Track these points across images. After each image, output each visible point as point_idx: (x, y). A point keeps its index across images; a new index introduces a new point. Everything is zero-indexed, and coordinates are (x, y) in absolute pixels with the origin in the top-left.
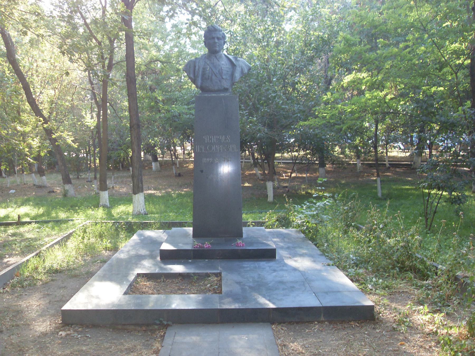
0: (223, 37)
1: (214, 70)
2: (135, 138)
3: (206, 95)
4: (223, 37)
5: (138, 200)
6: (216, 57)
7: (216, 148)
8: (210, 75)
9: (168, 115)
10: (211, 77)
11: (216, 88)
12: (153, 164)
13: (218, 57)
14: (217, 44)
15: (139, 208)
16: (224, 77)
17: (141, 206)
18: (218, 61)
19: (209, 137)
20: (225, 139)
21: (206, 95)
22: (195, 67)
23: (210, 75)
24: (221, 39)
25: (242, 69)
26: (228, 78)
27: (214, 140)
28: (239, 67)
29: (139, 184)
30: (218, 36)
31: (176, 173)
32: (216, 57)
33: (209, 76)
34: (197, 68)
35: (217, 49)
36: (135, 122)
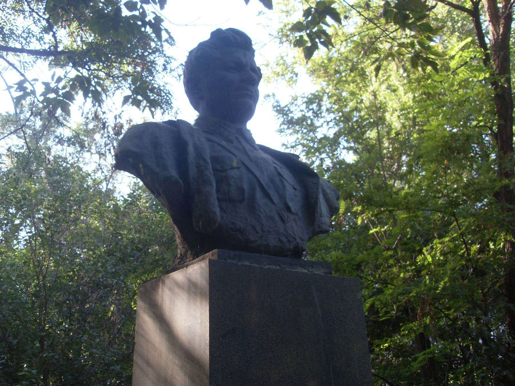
10: (252, 198)
11: (272, 241)
33: (241, 190)
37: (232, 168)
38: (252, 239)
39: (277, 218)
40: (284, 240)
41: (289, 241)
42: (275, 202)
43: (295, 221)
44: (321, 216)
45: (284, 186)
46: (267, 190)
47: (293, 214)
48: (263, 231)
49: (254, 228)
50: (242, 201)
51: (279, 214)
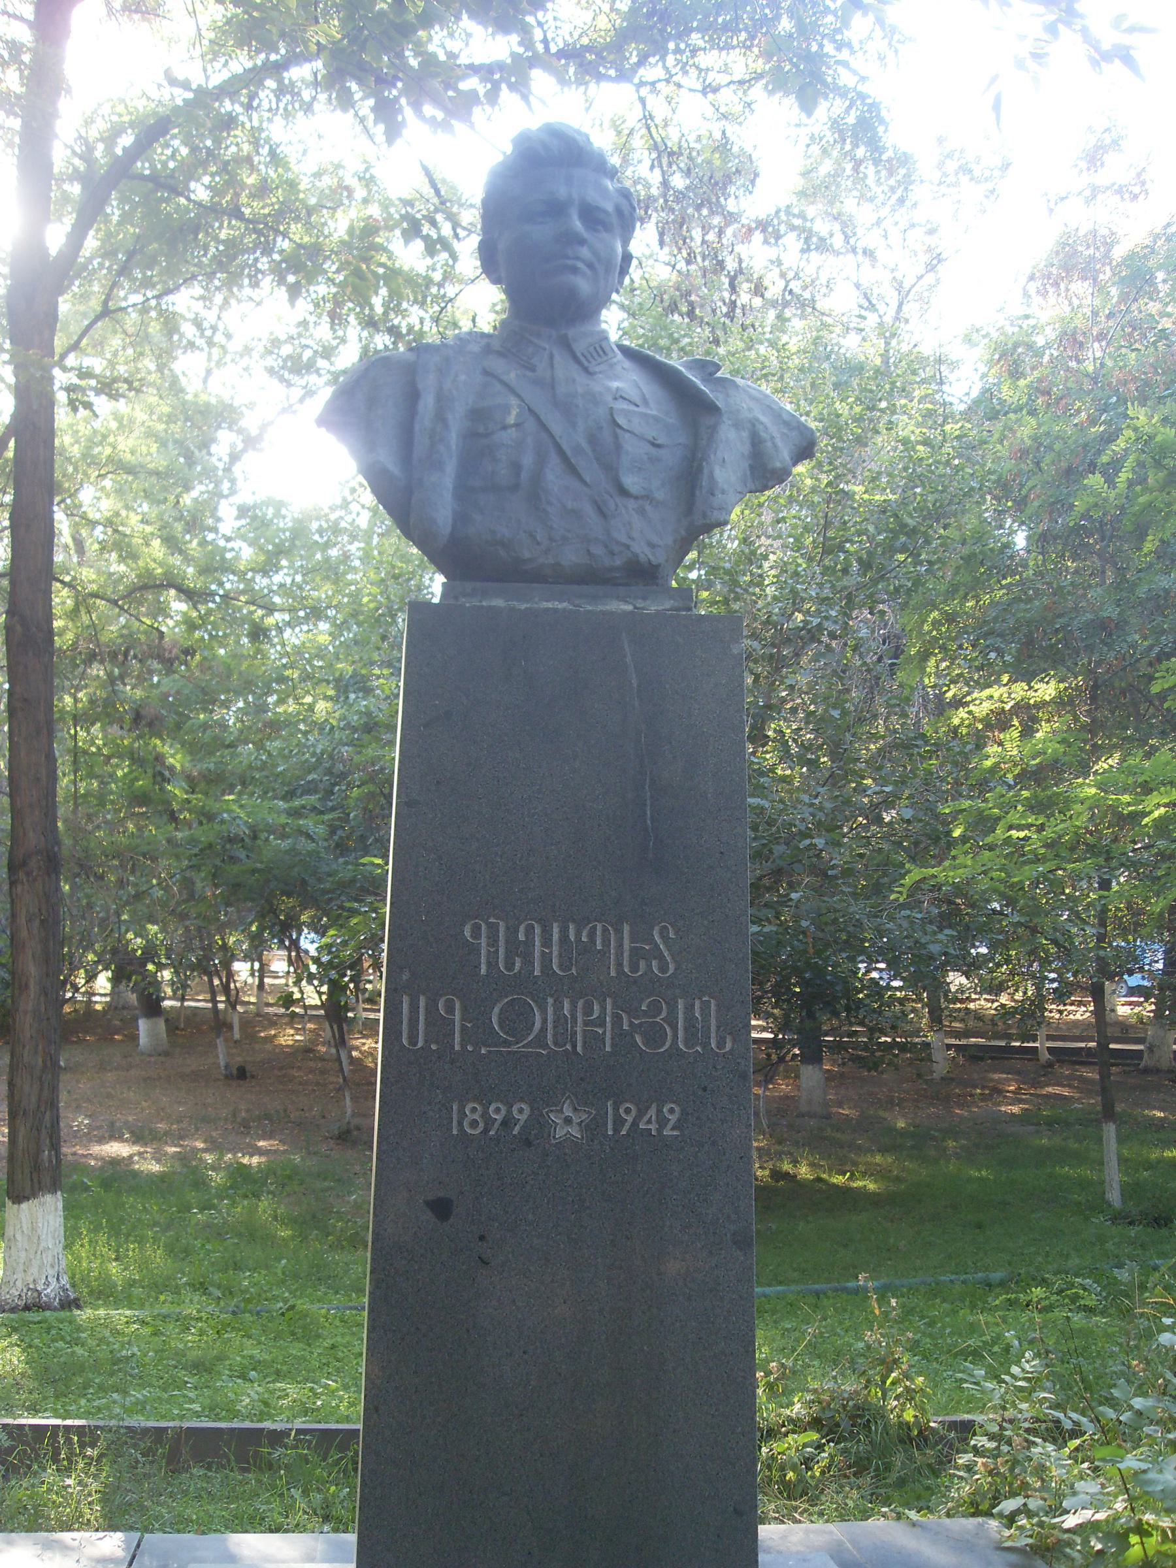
0: (619, 212)
1: (557, 427)
2: (29, 920)
3: (499, 603)
4: (619, 212)
5: (33, 1229)
6: (566, 345)
7: (559, 1020)
8: (528, 460)
9: (205, 834)
10: (537, 478)
11: (571, 557)
12: (143, 1025)
13: (579, 347)
14: (585, 252)
15: (34, 1270)
16: (631, 481)
17: (48, 1258)
18: (586, 370)
19: (512, 931)
21: (499, 603)
22: (413, 396)
23: (528, 460)
24: (608, 228)
25: (756, 441)
26: (660, 495)
27: (546, 959)
28: (737, 425)
29: (39, 1151)
30: (593, 197)
31: (226, 1067)
32: (566, 345)
33: (516, 467)
34: (427, 403)
35: (583, 285)
36: (33, 839)
37: (505, 428)
38: (527, 555)
39: (589, 510)
40: (598, 550)
41: (612, 553)
42: (588, 479)
43: (642, 512)
44: (713, 494)
45: (618, 447)
46: (573, 461)
47: (636, 498)
48: (551, 539)
49: (531, 536)
50: (515, 488)
51: (595, 502)
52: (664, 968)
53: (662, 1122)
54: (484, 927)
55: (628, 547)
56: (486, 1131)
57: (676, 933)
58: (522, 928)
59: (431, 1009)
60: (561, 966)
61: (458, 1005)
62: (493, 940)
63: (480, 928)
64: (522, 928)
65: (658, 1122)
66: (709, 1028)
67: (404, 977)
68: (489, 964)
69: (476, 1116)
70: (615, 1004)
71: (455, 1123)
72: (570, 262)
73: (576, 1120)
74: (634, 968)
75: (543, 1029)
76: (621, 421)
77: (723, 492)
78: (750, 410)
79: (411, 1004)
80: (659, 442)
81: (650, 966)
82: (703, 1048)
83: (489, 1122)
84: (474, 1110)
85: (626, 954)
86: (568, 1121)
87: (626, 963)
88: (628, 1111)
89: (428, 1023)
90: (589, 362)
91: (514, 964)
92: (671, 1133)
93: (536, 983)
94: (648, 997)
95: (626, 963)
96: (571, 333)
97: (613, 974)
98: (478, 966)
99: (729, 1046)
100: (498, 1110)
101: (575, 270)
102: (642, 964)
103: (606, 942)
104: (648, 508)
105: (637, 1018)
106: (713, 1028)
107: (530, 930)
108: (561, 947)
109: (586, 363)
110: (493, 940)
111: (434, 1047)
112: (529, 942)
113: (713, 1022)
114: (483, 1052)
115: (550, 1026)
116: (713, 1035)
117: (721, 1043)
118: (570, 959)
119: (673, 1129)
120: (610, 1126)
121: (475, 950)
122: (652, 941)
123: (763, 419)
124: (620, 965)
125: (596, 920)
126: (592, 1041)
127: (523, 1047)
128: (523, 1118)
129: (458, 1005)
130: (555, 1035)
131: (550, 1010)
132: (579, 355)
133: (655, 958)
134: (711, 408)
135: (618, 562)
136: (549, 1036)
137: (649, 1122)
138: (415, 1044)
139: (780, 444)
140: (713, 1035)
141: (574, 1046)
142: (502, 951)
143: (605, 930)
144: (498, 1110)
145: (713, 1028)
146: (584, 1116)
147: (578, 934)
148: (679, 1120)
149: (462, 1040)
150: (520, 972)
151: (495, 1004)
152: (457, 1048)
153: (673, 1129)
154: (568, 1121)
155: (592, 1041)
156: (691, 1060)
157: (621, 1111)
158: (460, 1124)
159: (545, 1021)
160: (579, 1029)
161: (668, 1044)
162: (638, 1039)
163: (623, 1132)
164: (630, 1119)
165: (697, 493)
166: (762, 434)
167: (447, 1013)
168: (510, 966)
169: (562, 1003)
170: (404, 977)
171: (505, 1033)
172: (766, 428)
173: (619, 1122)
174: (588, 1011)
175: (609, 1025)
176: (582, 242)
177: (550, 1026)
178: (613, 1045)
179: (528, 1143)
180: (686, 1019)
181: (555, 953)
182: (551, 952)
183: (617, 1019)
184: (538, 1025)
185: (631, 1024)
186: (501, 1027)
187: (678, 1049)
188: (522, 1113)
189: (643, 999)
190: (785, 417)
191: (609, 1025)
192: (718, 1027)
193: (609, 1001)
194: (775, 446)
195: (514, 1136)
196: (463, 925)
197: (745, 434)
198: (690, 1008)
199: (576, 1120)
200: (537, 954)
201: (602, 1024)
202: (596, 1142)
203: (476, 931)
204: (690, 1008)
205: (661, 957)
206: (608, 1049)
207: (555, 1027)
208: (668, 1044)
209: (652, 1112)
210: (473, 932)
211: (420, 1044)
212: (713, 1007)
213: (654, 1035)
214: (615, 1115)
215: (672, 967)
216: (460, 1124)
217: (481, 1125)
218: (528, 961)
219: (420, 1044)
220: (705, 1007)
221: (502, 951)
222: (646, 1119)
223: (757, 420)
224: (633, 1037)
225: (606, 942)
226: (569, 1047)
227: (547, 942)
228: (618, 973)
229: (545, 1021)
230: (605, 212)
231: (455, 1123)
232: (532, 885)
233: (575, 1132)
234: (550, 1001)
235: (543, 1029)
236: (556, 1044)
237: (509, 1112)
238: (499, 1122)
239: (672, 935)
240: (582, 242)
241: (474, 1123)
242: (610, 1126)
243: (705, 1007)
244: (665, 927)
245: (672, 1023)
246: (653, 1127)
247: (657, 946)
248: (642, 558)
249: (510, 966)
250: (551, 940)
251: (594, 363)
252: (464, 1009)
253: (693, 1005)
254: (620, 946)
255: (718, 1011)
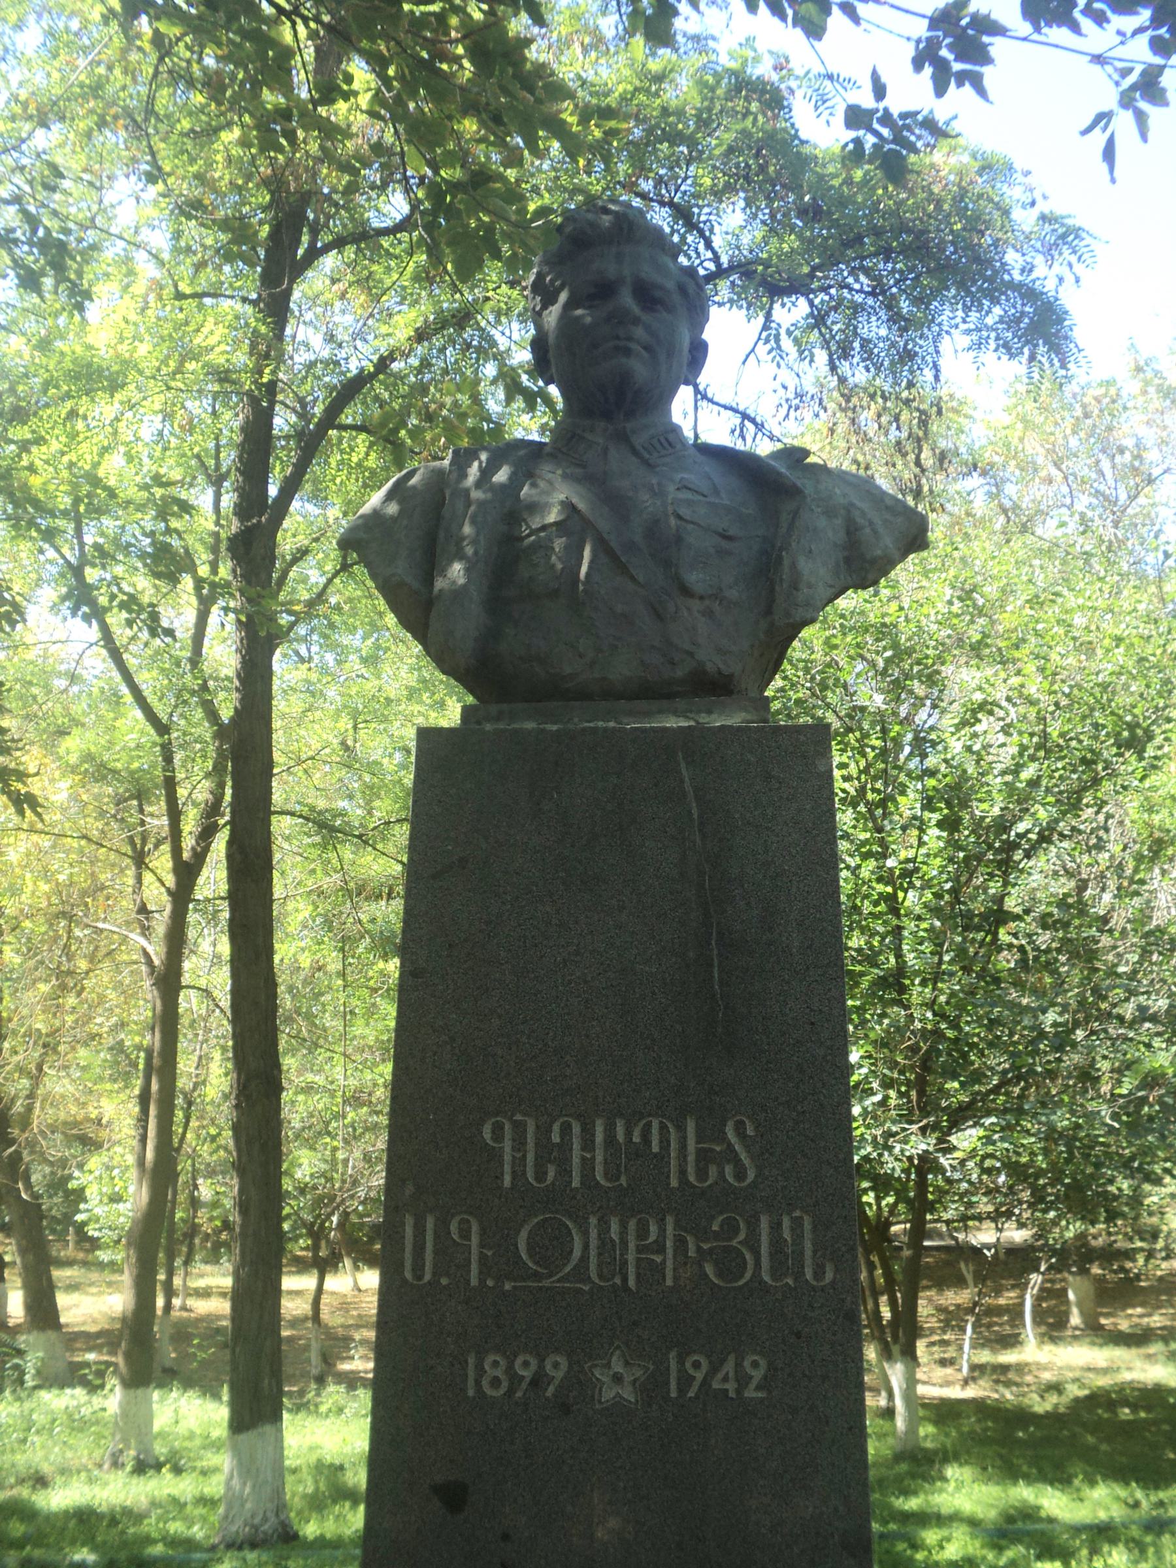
6: (623, 438)
11: (622, 669)
13: (639, 441)
14: (639, 332)
16: (694, 578)
18: (649, 465)
19: (544, 1131)
20: (704, 1157)
21: (530, 725)
25: (851, 529)
26: (733, 594)
27: (588, 1166)
28: (830, 513)
30: (648, 272)
32: (623, 438)
35: (639, 369)
38: (568, 670)
41: (672, 663)
42: (641, 578)
43: (709, 613)
44: (796, 589)
45: (679, 539)
52: (740, 1175)
53: (743, 1380)
54: (507, 1127)
55: (691, 654)
56: (510, 1392)
57: (756, 1128)
58: (556, 1127)
59: (442, 1233)
60: (606, 1175)
61: (475, 1228)
62: (520, 1143)
63: (502, 1128)
64: (556, 1127)
65: (737, 1380)
66: (802, 1253)
67: (407, 1193)
68: (514, 1172)
69: (499, 1373)
70: (677, 1225)
71: (471, 1382)
72: (622, 343)
73: (628, 1379)
74: (702, 1174)
75: (584, 1258)
76: (684, 512)
77: (810, 586)
78: (845, 495)
79: (416, 1226)
80: (731, 533)
81: (721, 1174)
82: (796, 1280)
83: (515, 1379)
84: (495, 1364)
85: (691, 1158)
86: (618, 1379)
87: (691, 1169)
88: (697, 1365)
89: (436, 1252)
90: (650, 453)
91: (546, 1173)
92: (754, 1395)
93: (574, 1198)
94: (721, 1213)
95: (691, 1169)
96: (629, 426)
97: (674, 1183)
98: (499, 1177)
99: (829, 1276)
100: (526, 1364)
101: (628, 352)
102: (713, 1171)
103: (665, 1143)
104: (716, 607)
105: (707, 1240)
106: (808, 1253)
107: (566, 1130)
108: (606, 1150)
109: (647, 456)
110: (520, 1143)
111: (444, 1281)
112: (565, 1146)
113: (808, 1246)
114: (507, 1286)
115: (593, 1253)
116: (808, 1261)
117: (819, 1273)
118: (619, 1166)
119: (758, 1388)
120: (673, 1385)
121: (495, 1156)
122: (723, 1138)
123: (858, 503)
124: (683, 1172)
125: (650, 1115)
126: (651, 1272)
127: (559, 1281)
128: (559, 1374)
129: (475, 1228)
130: (599, 1265)
131: (593, 1233)
132: (639, 448)
133: (728, 1162)
134: (793, 492)
135: (679, 673)
136: (593, 1266)
137: (725, 1379)
138: (420, 1278)
139: (881, 530)
140: (808, 1261)
141: (625, 1279)
142: (530, 1157)
143: (663, 1127)
144: (526, 1364)
145: (808, 1253)
146: (639, 1373)
147: (629, 1133)
148: (765, 1377)
149: (481, 1273)
150: (553, 1184)
151: (522, 1226)
152: (474, 1282)
153: (758, 1388)
154: (618, 1379)
155: (651, 1272)
156: (779, 1296)
157: (688, 1365)
158: (478, 1383)
159: (586, 1247)
160: (631, 1257)
161: (748, 1275)
162: (709, 1269)
163: (691, 1394)
164: (699, 1376)
165: (777, 588)
166: (860, 521)
167: (461, 1237)
168: (540, 1175)
169: (607, 1223)
170: (407, 1193)
171: (537, 1263)
172: (863, 513)
173: (685, 1380)
174: (642, 1233)
175: (670, 1252)
176: (636, 321)
177: (593, 1253)
178: (676, 1278)
179: (566, 1409)
180: (771, 1244)
181: (599, 1158)
182: (593, 1158)
183: (680, 1243)
184: (577, 1253)
185: (699, 1249)
186: (531, 1256)
187: (761, 1282)
188: (557, 1367)
189: (713, 1218)
190: (889, 502)
191: (670, 1252)
192: (815, 1252)
193: (670, 1220)
194: (875, 532)
195: (547, 1399)
196: (482, 1122)
197: (839, 521)
198: (776, 1227)
199: (628, 1379)
200: (576, 1161)
201: (661, 1249)
202: (655, 1407)
203: (498, 1130)
204: (776, 1227)
205: (737, 1162)
206: (669, 1282)
207: (600, 1254)
208: (748, 1275)
209: (729, 1366)
210: (493, 1132)
211: (427, 1277)
212: (807, 1226)
213: (730, 1263)
214: (679, 1371)
215: (751, 1175)
216: (478, 1383)
217: (505, 1385)
218: (565, 1171)
219: (427, 1277)
220: (797, 1224)
221: (530, 1157)
222: (720, 1376)
223: (852, 505)
224: (701, 1267)
225: (665, 1143)
226: (618, 1281)
227: (588, 1144)
228: (680, 1183)
229: (586, 1247)
230: (661, 288)
231: (471, 1382)
232: (568, 1072)
233: (628, 1394)
234: (593, 1221)
235: (584, 1258)
236: (600, 1276)
237: (541, 1367)
238: (528, 1380)
239: (750, 1131)
240: (636, 321)
241: (495, 1383)
242: (673, 1385)
243: (797, 1224)
244: (742, 1122)
245: (753, 1244)
246: (731, 1386)
247: (730, 1145)
248: (709, 667)
249: (540, 1175)
250: (593, 1142)
251: (656, 454)
252: (483, 1232)
253: (780, 1224)
254: (683, 1146)
255: (815, 1228)
